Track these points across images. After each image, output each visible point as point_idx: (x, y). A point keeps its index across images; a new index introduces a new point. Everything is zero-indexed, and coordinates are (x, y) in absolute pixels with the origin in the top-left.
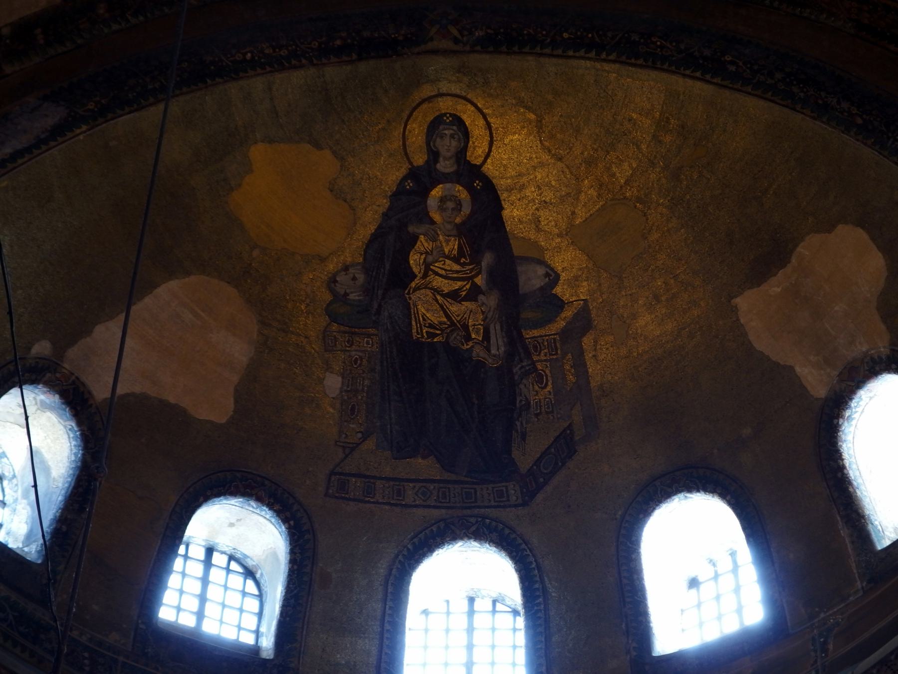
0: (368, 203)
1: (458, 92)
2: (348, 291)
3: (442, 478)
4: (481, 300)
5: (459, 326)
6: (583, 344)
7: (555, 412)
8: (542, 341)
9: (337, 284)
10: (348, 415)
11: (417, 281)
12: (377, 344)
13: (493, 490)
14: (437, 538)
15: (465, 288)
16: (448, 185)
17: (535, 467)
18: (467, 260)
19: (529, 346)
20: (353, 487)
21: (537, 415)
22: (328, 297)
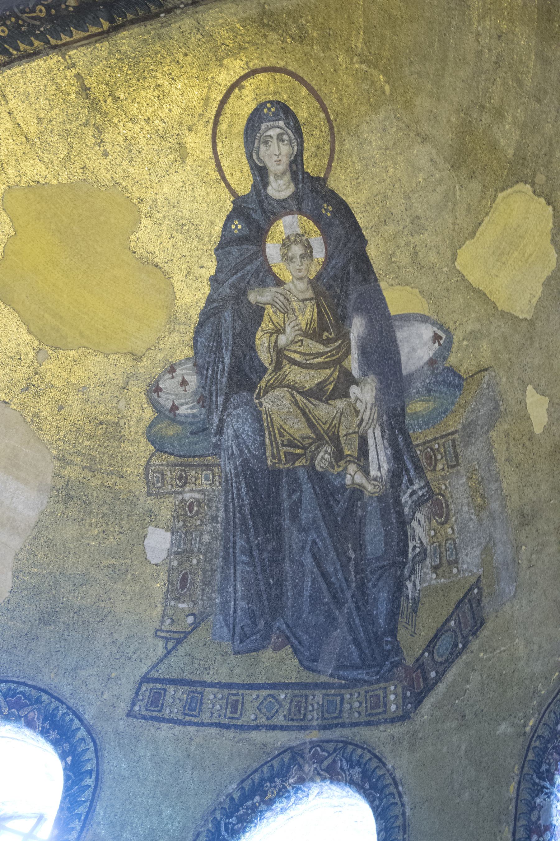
0: (187, 264)
1: (273, 62)
2: (176, 403)
3: (298, 681)
5: (327, 439)
8: (436, 446)
11: (267, 377)
12: (220, 478)
13: (366, 696)
14: (276, 779)
15: (332, 379)
16: (288, 219)
17: (426, 654)
19: (420, 457)
20: (171, 700)
21: (435, 569)
22: (149, 414)
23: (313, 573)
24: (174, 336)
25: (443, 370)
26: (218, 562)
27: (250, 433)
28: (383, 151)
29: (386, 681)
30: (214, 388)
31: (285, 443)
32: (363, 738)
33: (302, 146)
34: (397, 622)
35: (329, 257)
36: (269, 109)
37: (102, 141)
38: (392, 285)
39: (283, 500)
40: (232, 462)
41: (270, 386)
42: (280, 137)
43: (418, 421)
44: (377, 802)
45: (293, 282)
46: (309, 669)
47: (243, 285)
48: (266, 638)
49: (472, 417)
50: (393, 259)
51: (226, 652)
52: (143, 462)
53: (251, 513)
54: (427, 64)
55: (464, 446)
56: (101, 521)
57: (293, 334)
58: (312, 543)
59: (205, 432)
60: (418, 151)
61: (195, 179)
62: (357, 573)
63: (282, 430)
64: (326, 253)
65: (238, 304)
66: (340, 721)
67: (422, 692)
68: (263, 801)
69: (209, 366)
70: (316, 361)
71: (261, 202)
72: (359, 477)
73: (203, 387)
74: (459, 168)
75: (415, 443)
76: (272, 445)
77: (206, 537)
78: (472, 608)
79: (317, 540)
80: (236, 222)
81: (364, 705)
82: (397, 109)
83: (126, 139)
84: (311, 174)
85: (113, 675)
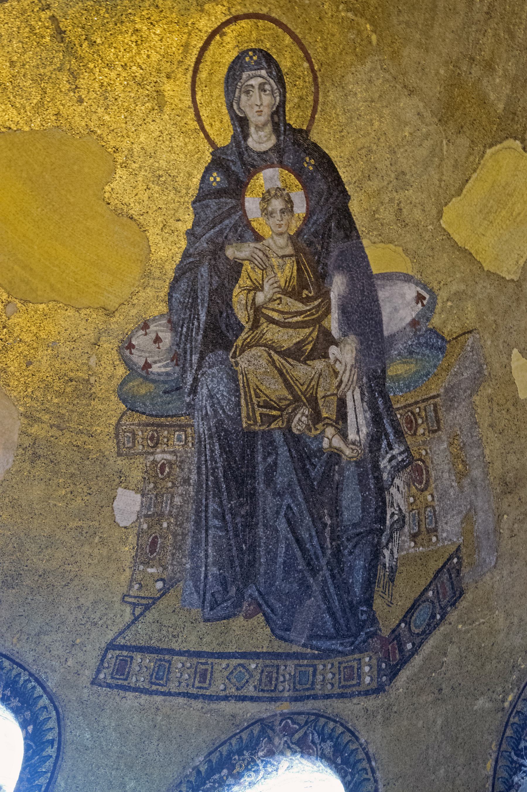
0: (163, 217)
2: (149, 360)
3: (270, 650)
5: (305, 401)
8: (417, 410)
9: (133, 351)
10: (146, 553)
11: (243, 335)
12: (193, 439)
13: (339, 667)
14: (245, 752)
15: (311, 339)
16: (269, 172)
17: (403, 625)
20: (138, 668)
21: (414, 537)
22: (121, 371)
23: (287, 539)
24: (148, 291)
25: (426, 331)
26: (190, 526)
28: (368, 103)
29: (361, 652)
30: (188, 345)
31: (261, 404)
32: (336, 711)
33: (285, 97)
34: (373, 592)
35: (310, 213)
36: (251, 58)
37: (77, 87)
38: (374, 243)
39: (257, 463)
40: (205, 423)
41: (246, 345)
42: (262, 87)
43: (399, 384)
44: (349, 778)
45: (272, 238)
46: (282, 638)
47: (220, 240)
48: (237, 605)
49: (455, 381)
50: (377, 216)
51: (196, 620)
52: (114, 421)
53: (224, 476)
54: (416, 14)
55: (445, 411)
56: (69, 481)
57: (271, 292)
58: (287, 508)
59: (178, 392)
60: (404, 104)
61: (173, 129)
62: (332, 540)
63: (258, 391)
64: (307, 209)
65: (215, 259)
66: (312, 692)
67: (397, 664)
68: (230, 774)
69: (184, 323)
70: (295, 319)
71: (241, 155)
72: (337, 441)
73: (177, 345)
74: (446, 122)
75: (395, 407)
76: (247, 405)
77: (177, 500)
78: (451, 578)
80: (215, 174)
81: (337, 676)
82: (384, 60)
83: (102, 85)
84: (294, 126)
85: (78, 641)
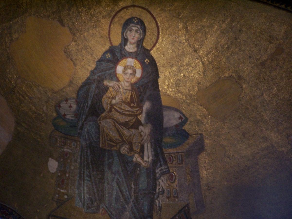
0: (84, 63)
1: (144, 6)
2: (66, 113)
4: (141, 129)
6: (198, 159)
7: (179, 197)
8: (174, 156)
9: (60, 108)
15: (132, 121)
18: (135, 105)
21: (168, 198)
22: (55, 115)
23: (117, 190)
27: (94, 133)
31: (109, 140)
35: (142, 77)
53: (91, 162)
57: (118, 101)
62: (134, 193)
65: (99, 83)
73: (78, 111)
76: (103, 138)
77: (72, 168)
79: (119, 178)
